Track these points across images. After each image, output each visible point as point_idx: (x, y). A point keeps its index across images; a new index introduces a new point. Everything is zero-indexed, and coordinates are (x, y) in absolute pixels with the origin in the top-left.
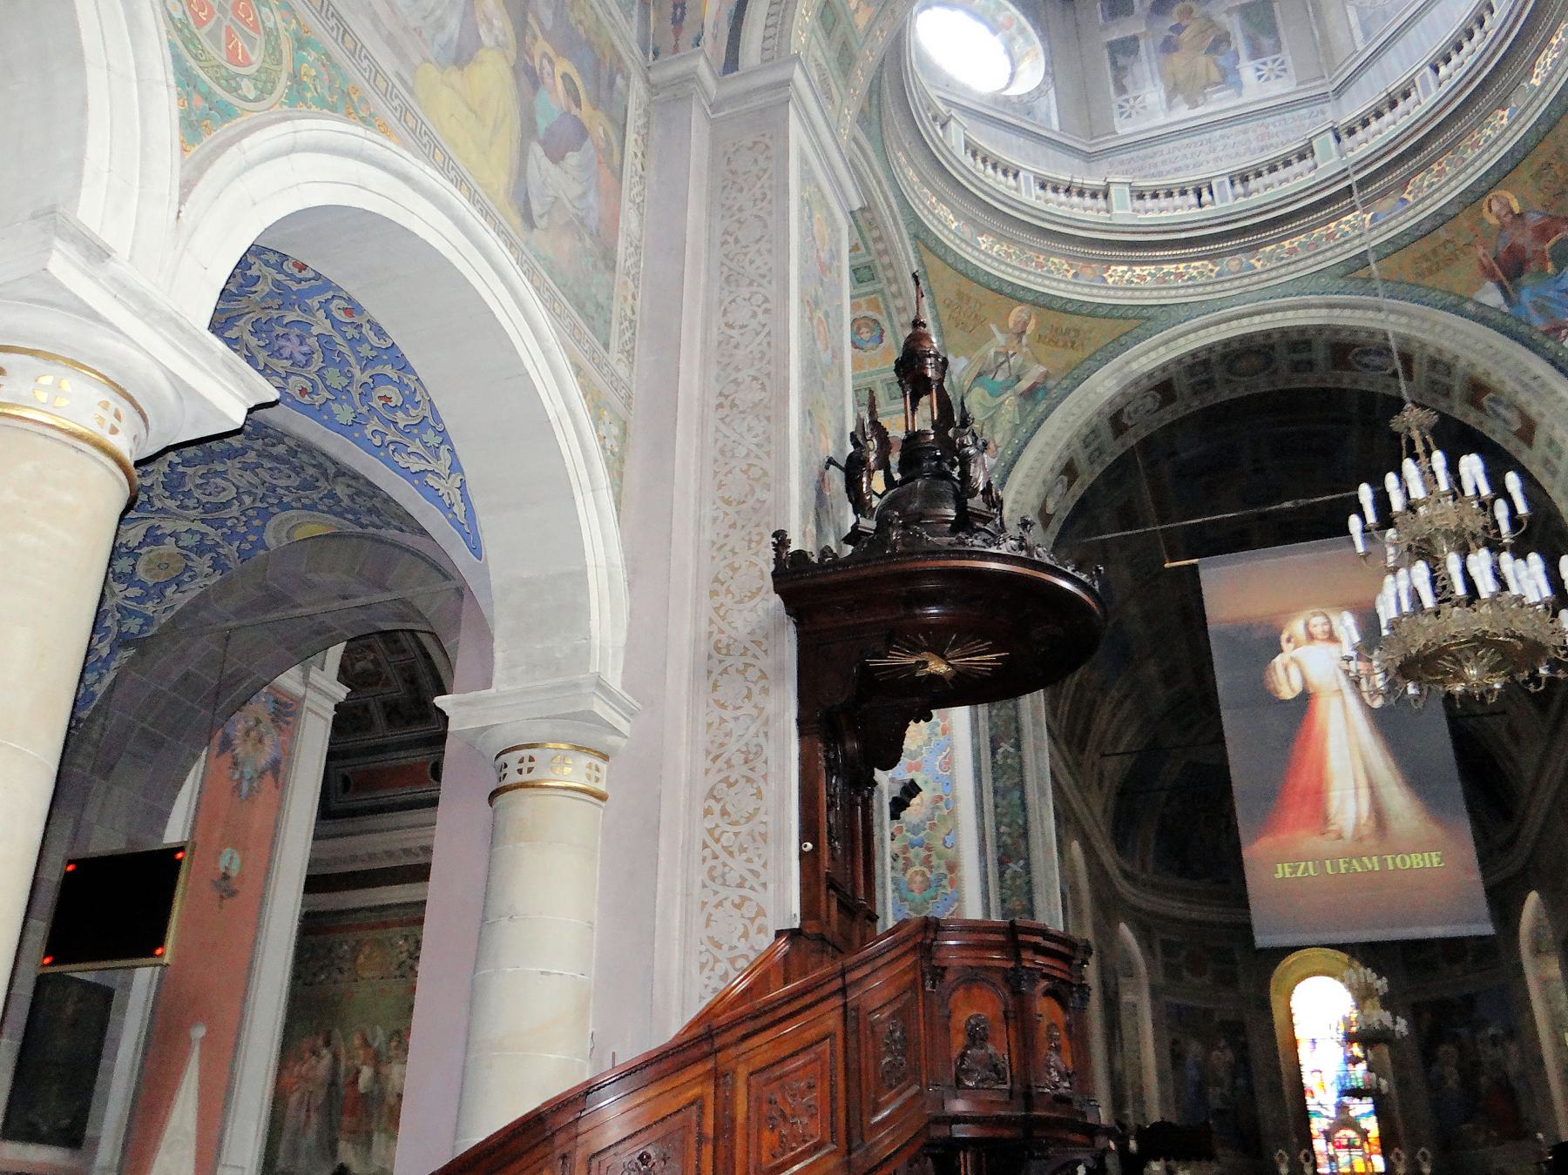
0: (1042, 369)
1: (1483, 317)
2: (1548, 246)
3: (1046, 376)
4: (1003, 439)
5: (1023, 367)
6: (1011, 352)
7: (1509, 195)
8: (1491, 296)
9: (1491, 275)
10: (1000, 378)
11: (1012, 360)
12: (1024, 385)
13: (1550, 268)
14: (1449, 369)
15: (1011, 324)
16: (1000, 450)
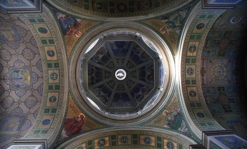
0: (162, 21)
1: (80, 18)
2: (70, 30)
3: (162, 20)
4: (176, 14)
5: (166, 23)
6: (167, 27)
7: (77, 36)
8: (78, 20)
9: (79, 24)
10: (171, 24)
11: (167, 26)
12: (167, 20)
13: (69, 26)
14: (85, 8)
15: (165, 32)
16: (177, 13)
